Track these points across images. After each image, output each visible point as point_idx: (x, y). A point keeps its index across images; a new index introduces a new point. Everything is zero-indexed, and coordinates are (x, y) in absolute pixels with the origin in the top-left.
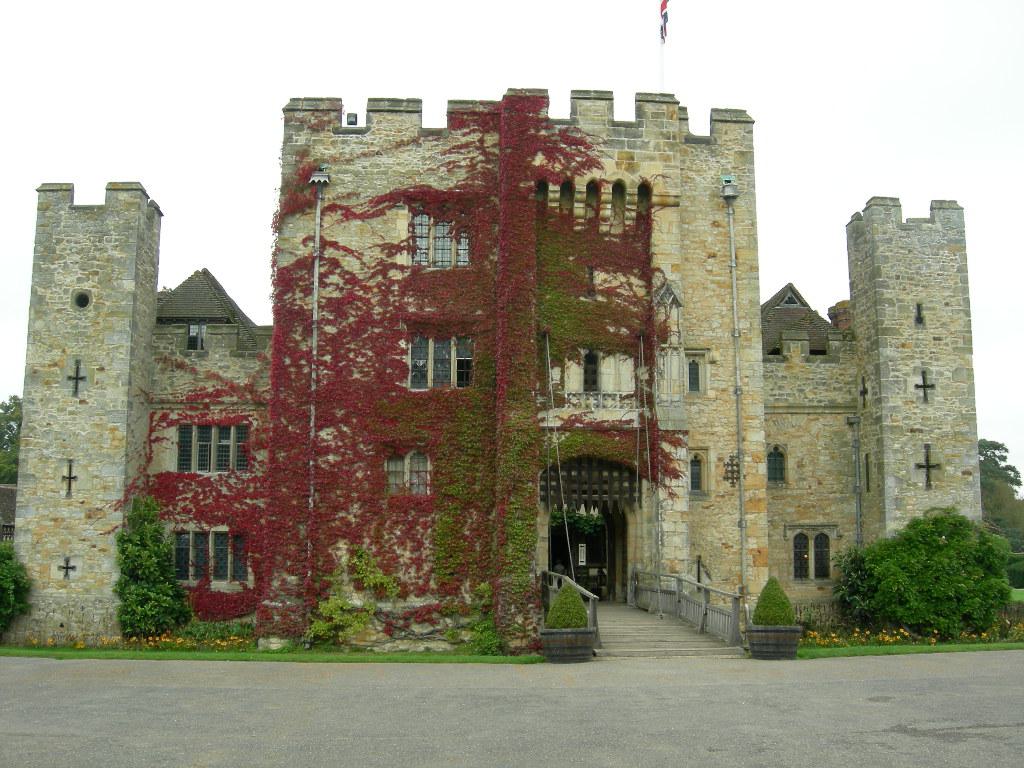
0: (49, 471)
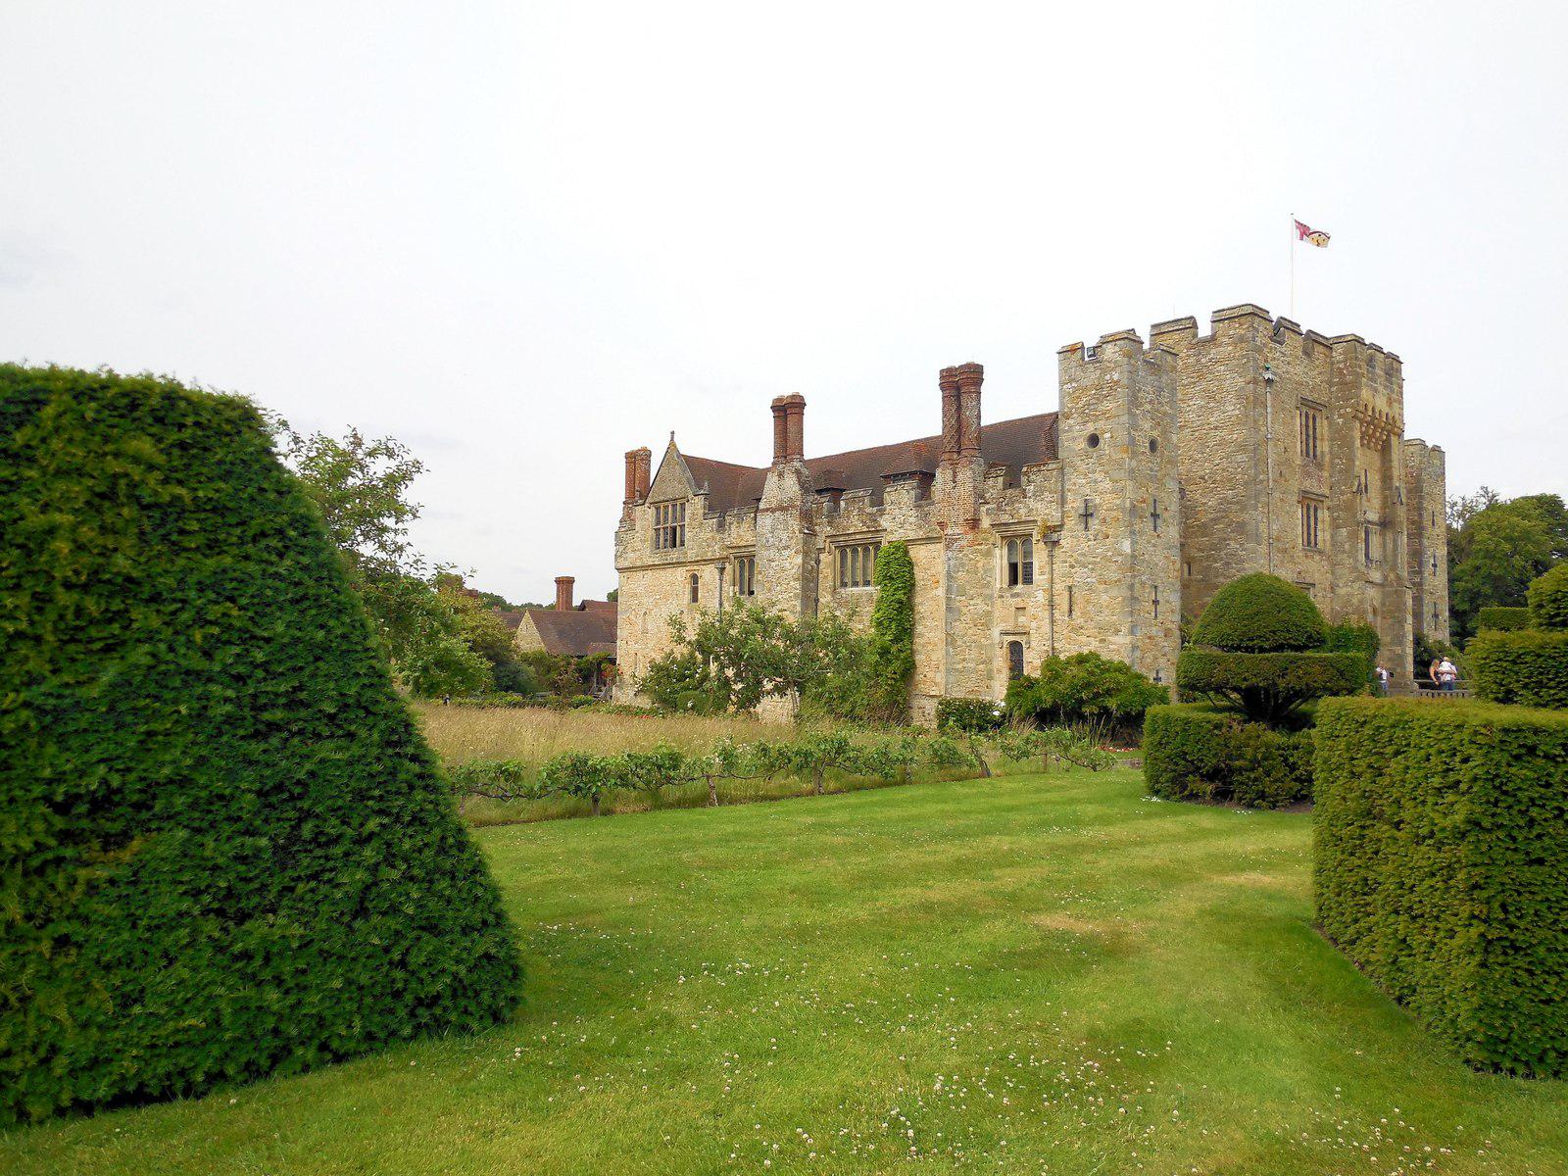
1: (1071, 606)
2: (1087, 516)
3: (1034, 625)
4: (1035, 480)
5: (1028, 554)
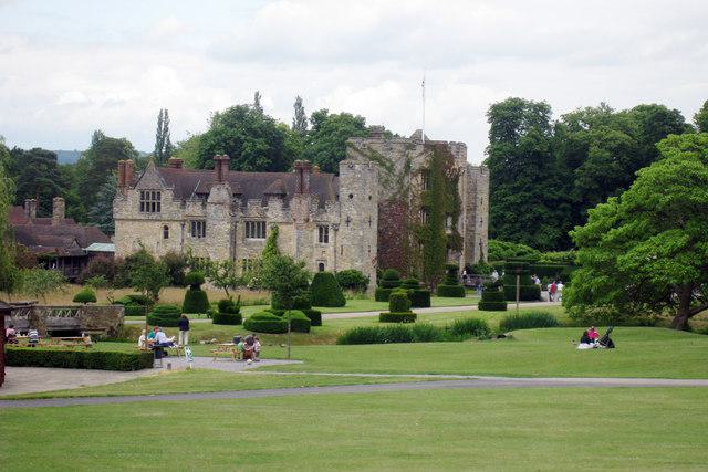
2: (348, 221)
5: (327, 232)
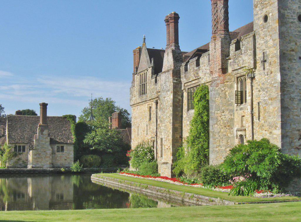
0: (295, 105)
1: (259, 114)
2: (265, 61)
3: (247, 125)
4: (246, 43)
